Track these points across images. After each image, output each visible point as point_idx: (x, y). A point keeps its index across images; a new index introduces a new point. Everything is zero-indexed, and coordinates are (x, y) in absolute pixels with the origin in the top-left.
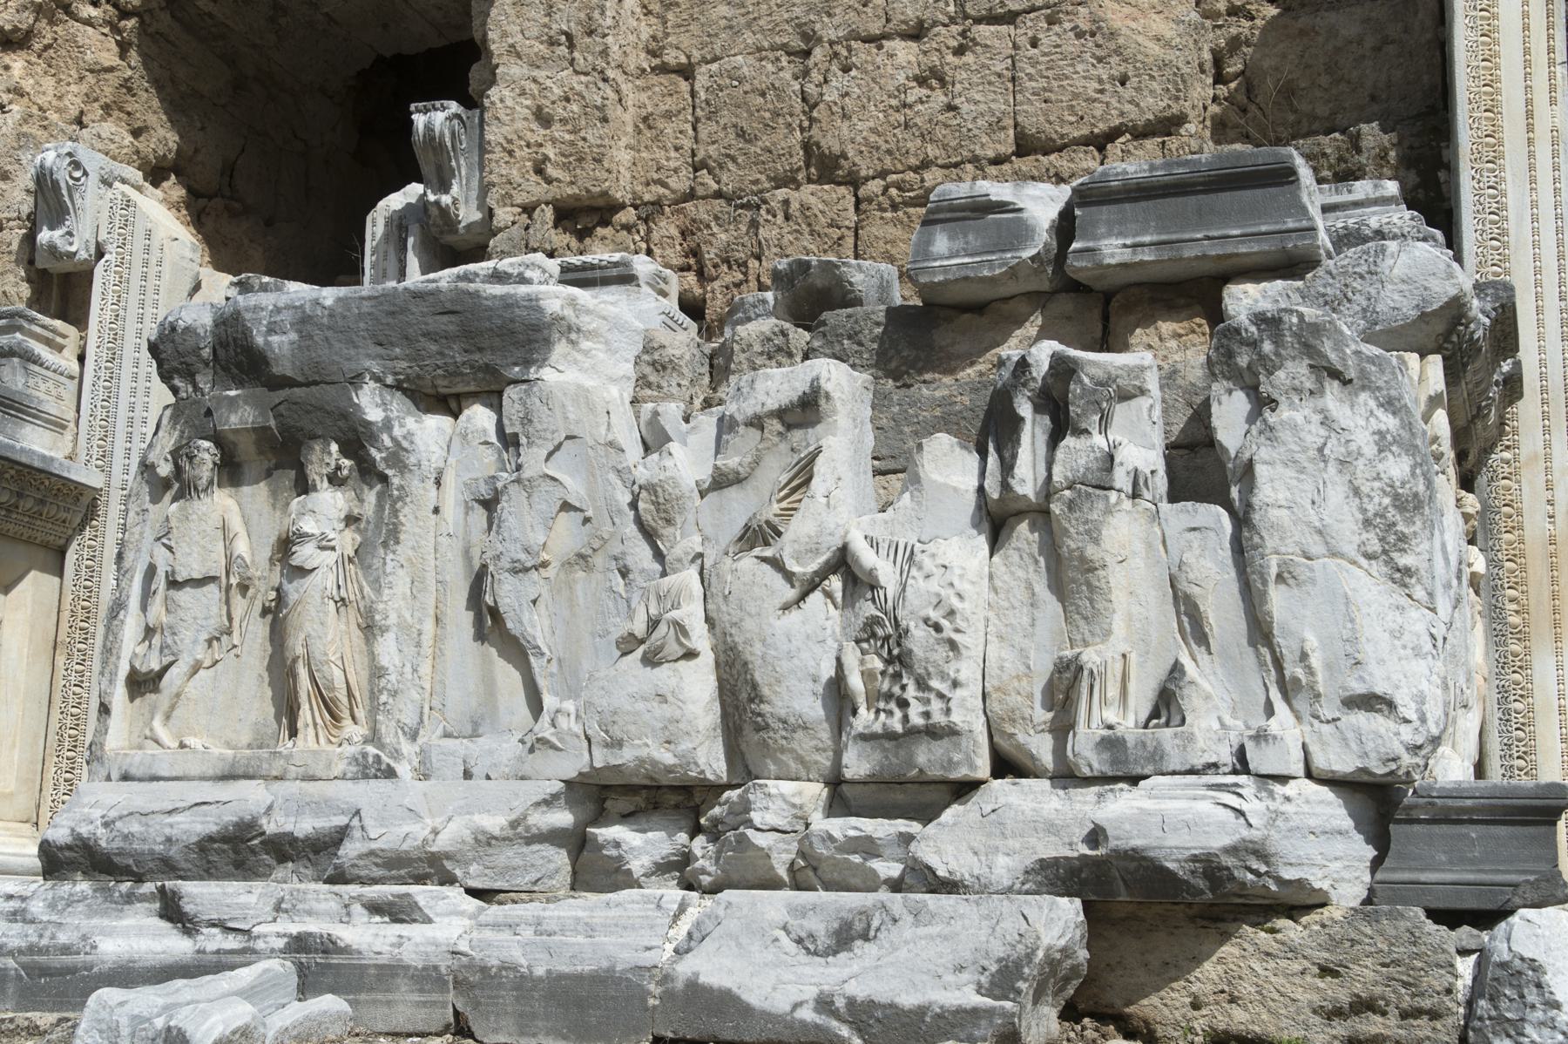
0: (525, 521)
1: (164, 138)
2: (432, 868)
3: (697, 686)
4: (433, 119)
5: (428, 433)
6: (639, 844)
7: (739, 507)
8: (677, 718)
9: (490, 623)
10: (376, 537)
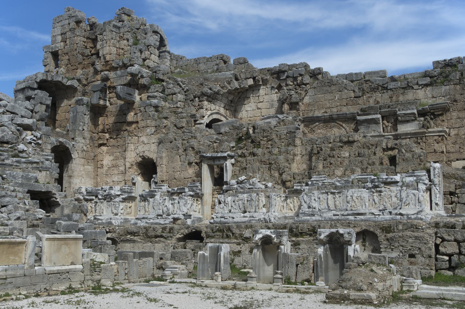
0: (155, 204)
1: (140, 172)
2: (151, 219)
3: (161, 211)
4: (154, 176)
5: (151, 200)
6: (159, 217)
7: (163, 203)
8: (160, 212)
9: (153, 208)
10: (149, 204)
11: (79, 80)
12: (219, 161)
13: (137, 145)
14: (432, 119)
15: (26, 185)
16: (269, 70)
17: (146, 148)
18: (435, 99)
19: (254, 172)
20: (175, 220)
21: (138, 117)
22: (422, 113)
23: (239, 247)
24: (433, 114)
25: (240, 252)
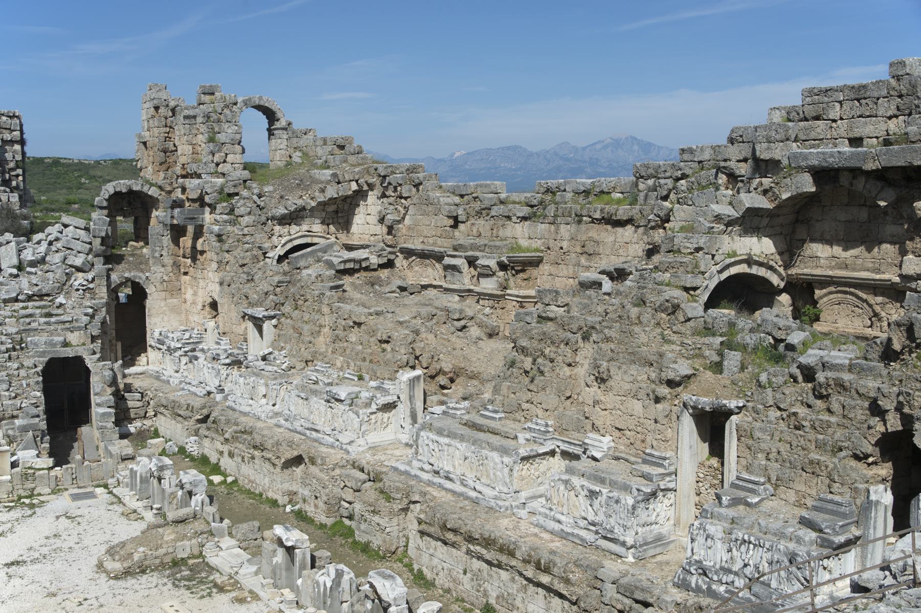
11: (161, 188)
14: (514, 275)
15: (49, 352)
18: (531, 241)
19: (286, 342)
20: (209, 393)
22: (503, 267)
24: (513, 268)
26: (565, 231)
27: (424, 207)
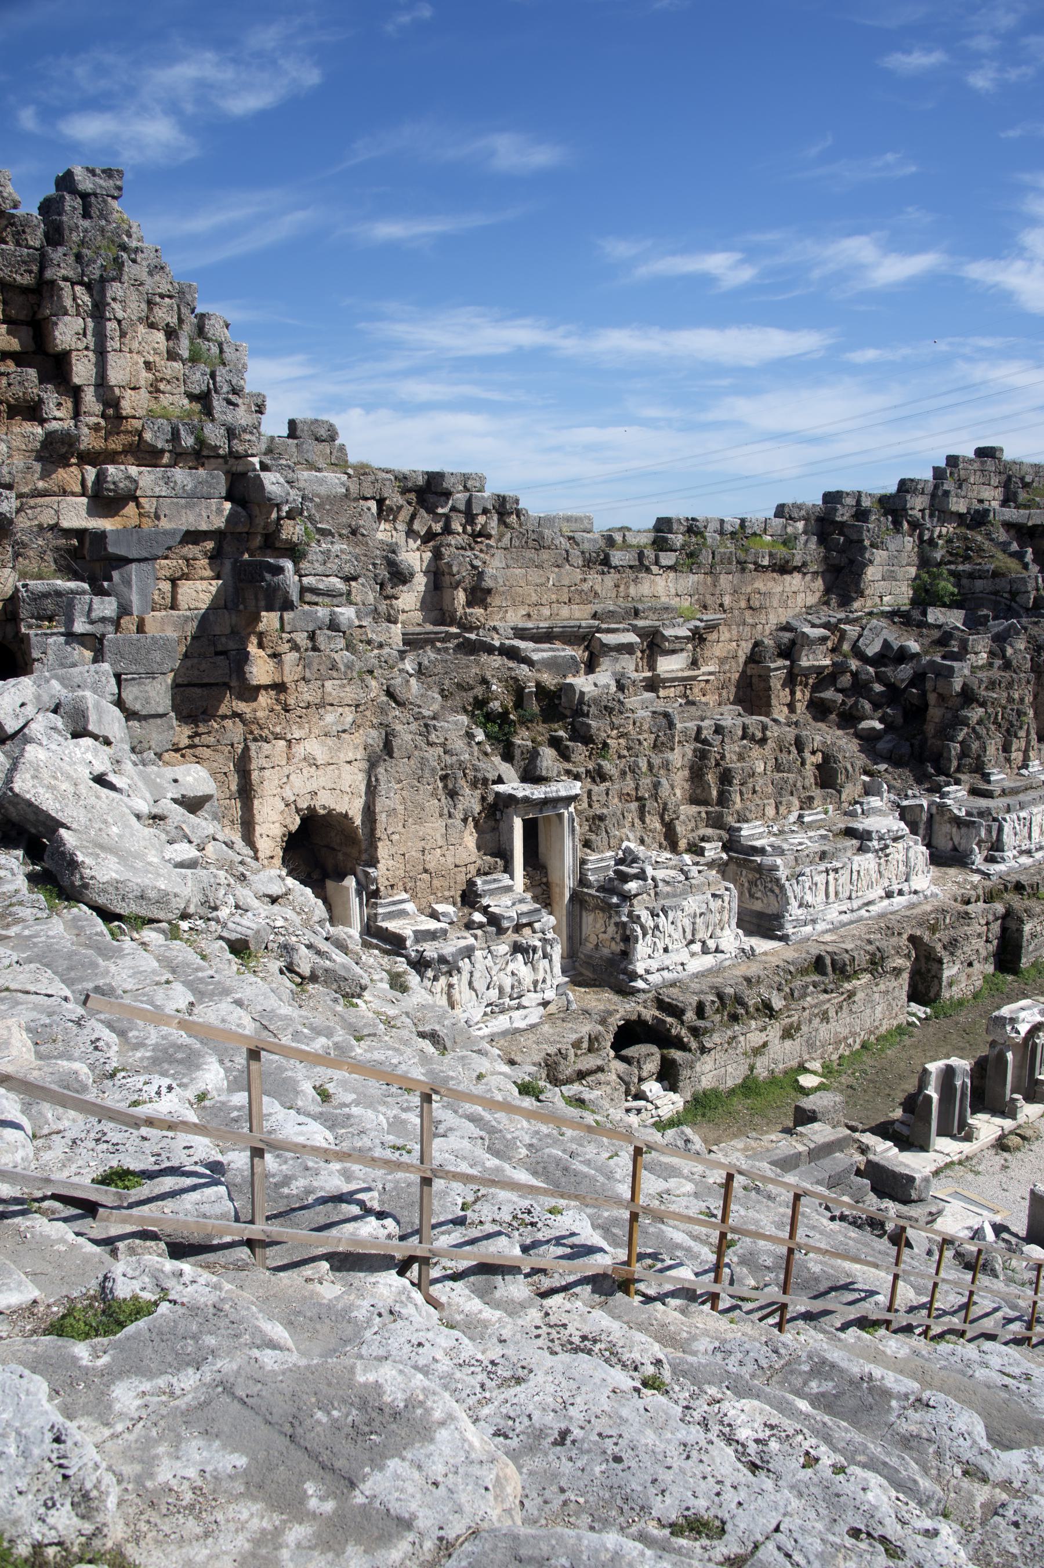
12: (555, 807)
13: (286, 770)
16: (401, 478)
17: (321, 779)
21: (287, 668)
23: (763, 1035)
25: (765, 1045)
26: (725, 581)
27: (530, 554)
